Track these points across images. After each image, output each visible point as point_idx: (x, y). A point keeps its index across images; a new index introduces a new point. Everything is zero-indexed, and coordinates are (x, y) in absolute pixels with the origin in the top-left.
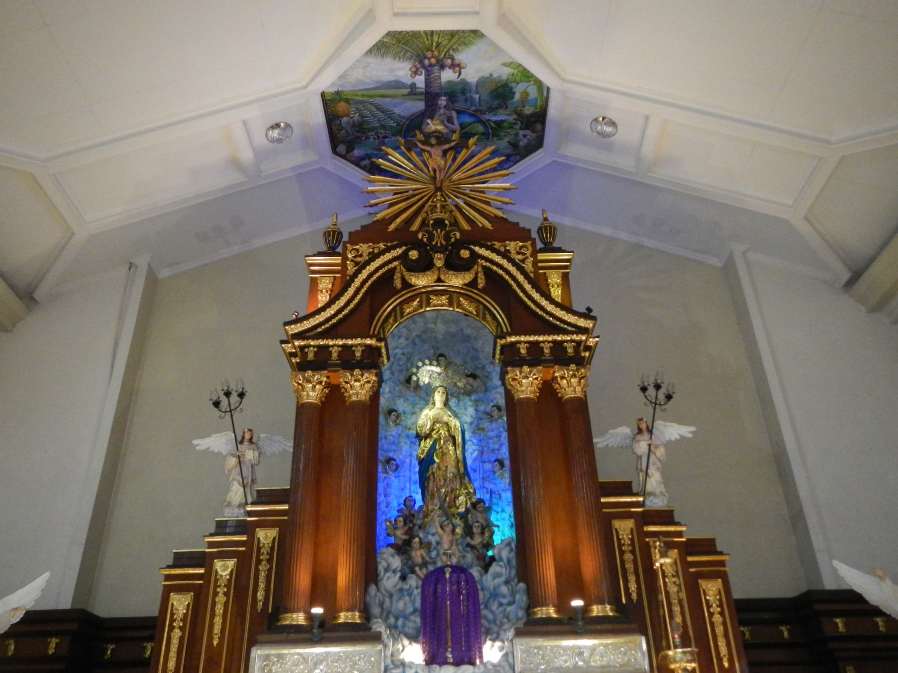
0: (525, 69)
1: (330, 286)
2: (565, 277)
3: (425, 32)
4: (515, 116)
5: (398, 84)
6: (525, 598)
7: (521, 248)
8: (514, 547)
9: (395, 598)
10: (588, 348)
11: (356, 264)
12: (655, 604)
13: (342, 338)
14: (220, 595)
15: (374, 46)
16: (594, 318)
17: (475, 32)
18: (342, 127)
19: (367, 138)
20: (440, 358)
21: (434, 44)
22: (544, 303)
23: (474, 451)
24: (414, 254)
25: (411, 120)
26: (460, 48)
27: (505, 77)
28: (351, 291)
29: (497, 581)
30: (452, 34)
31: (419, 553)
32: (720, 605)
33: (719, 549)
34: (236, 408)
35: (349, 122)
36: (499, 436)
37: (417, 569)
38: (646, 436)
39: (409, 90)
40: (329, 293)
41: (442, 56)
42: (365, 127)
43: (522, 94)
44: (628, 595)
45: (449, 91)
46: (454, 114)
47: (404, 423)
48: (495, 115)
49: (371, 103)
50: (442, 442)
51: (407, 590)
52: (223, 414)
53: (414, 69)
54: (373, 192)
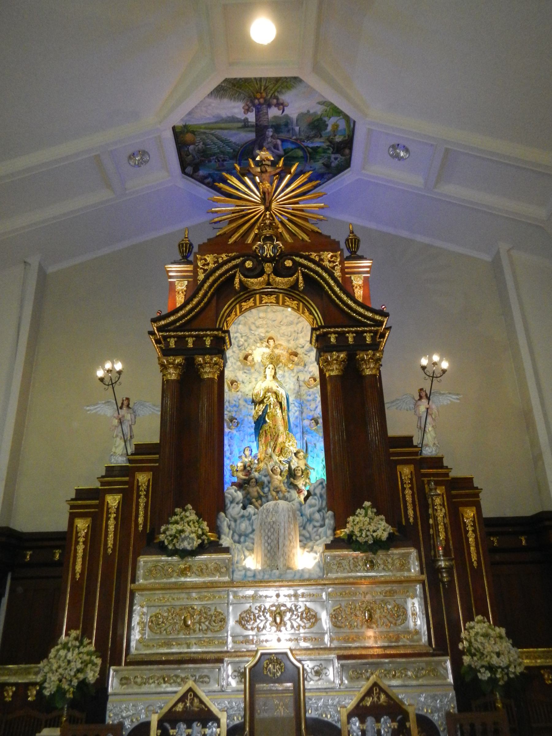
0: (336, 107)
1: (185, 289)
2: (366, 280)
3: (255, 79)
4: (328, 143)
5: (233, 119)
6: (332, 522)
7: (332, 257)
8: (325, 486)
9: (238, 522)
11: (205, 270)
12: (426, 526)
14: (112, 519)
15: (214, 90)
17: (295, 78)
18: (189, 153)
19: (210, 161)
20: (269, 340)
21: (263, 87)
23: (296, 411)
24: (249, 264)
25: (246, 147)
26: (284, 91)
27: (319, 113)
29: (312, 509)
30: (277, 80)
31: (255, 489)
32: (474, 526)
34: (116, 382)
35: (195, 149)
37: (254, 500)
38: (424, 401)
39: (243, 124)
40: (184, 293)
41: (269, 97)
42: (208, 153)
43: (333, 126)
44: (407, 519)
45: (274, 124)
46: (279, 142)
48: (312, 143)
49: (212, 134)
50: (272, 406)
51: (247, 517)
52: (107, 387)
53: (247, 108)
54: (216, 212)
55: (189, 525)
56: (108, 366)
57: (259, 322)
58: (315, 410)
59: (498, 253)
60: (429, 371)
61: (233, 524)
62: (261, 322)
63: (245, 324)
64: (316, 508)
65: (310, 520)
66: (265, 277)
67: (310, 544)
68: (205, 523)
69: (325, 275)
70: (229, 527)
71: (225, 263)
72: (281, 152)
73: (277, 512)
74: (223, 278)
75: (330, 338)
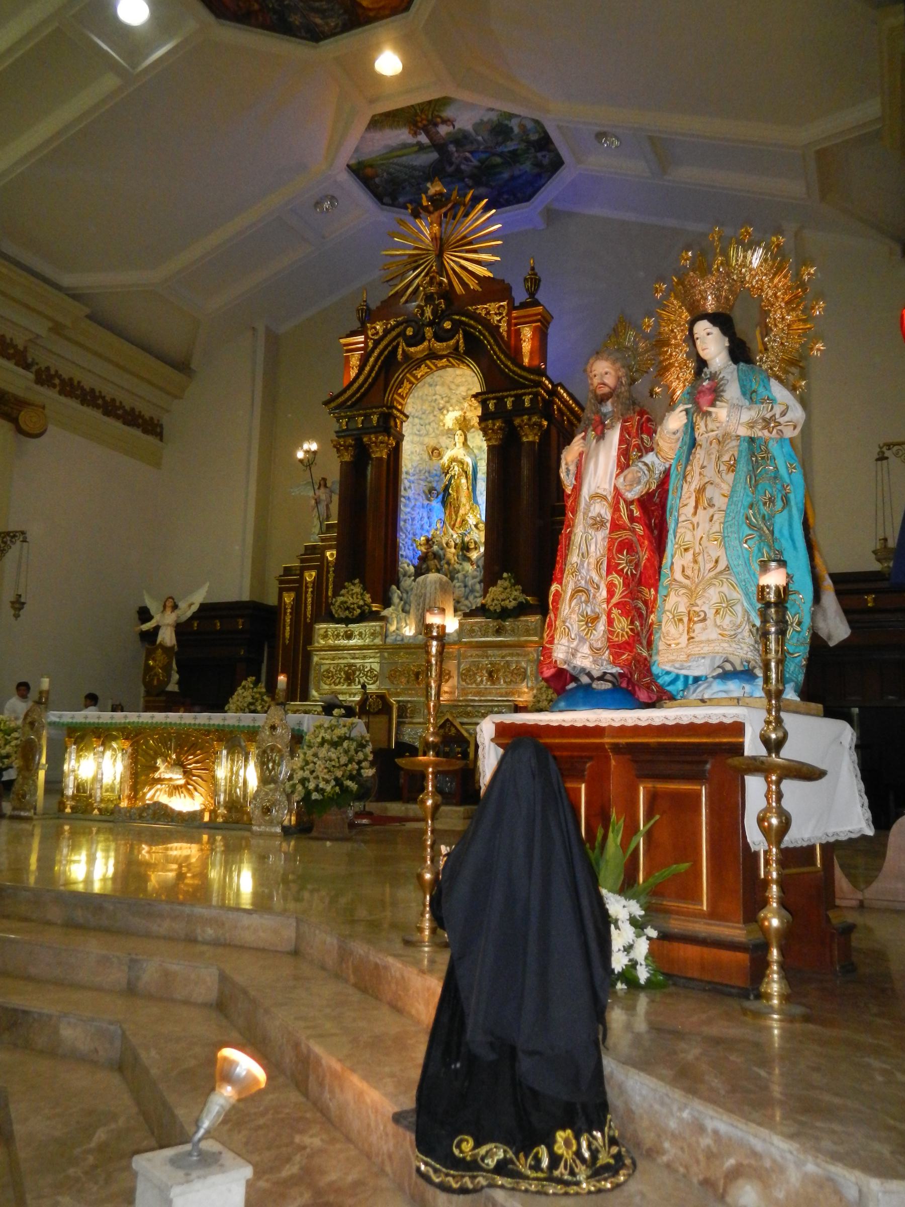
4: (525, 144)
5: (405, 146)
7: (499, 308)
19: (404, 188)
24: (410, 332)
27: (495, 118)
28: (367, 368)
29: (475, 580)
30: (430, 102)
31: (432, 562)
41: (430, 117)
46: (468, 154)
49: (391, 163)
50: (456, 477)
53: (412, 132)
55: (352, 598)
57: (458, 380)
61: (405, 596)
62: (460, 380)
63: (443, 385)
64: (478, 580)
65: (472, 591)
66: (426, 343)
68: (368, 596)
70: (401, 599)
71: (393, 328)
72: (475, 163)
73: (425, 584)
74: (390, 348)
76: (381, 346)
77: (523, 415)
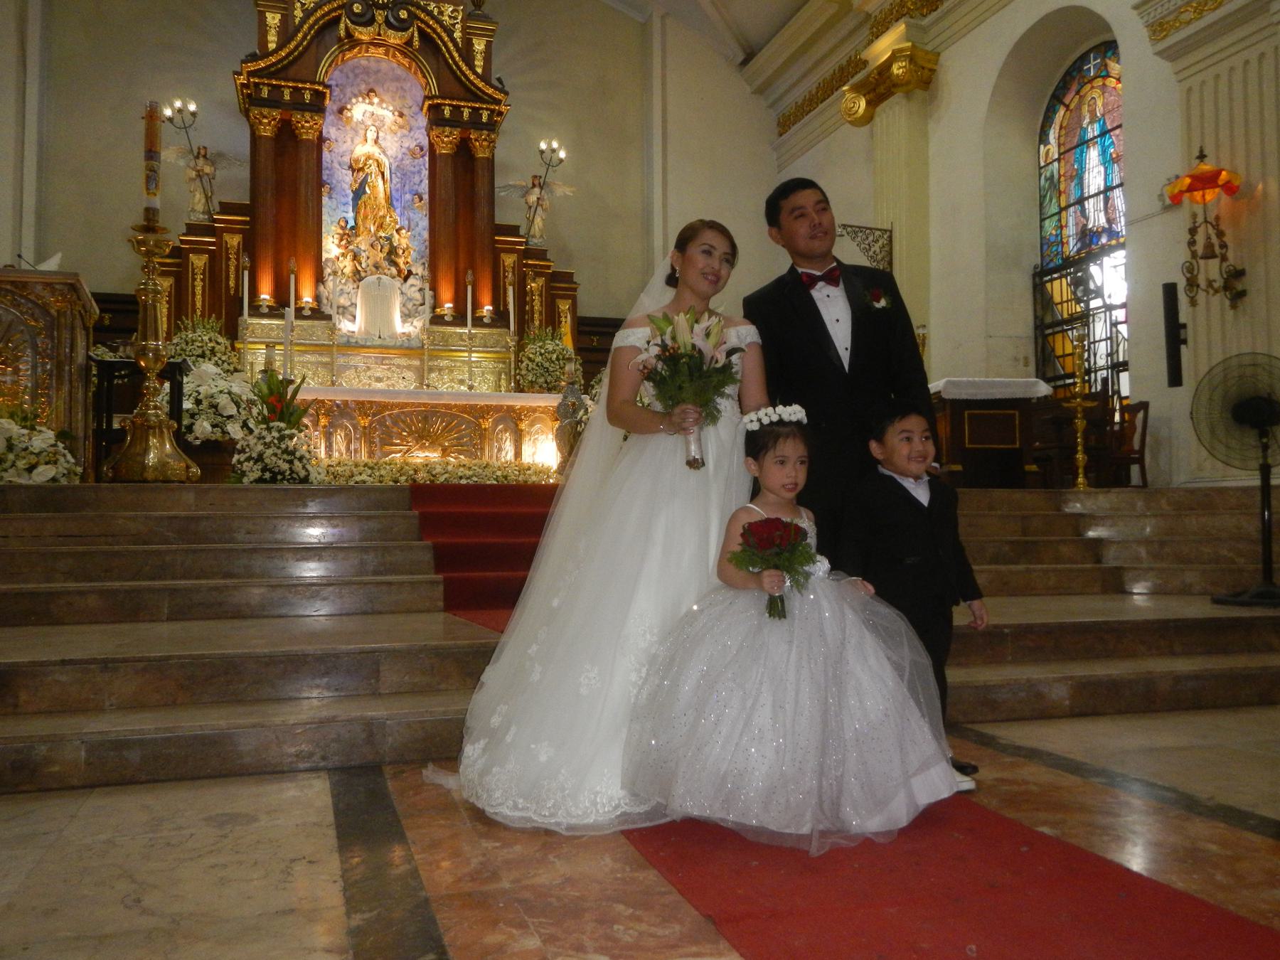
2: (489, 45)
7: (452, 12)
10: (500, 114)
13: (294, 81)
14: (198, 280)
16: (506, 93)
22: (468, 72)
24: (357, 8)
28: (300, 35)
33: (575, 280)
34: (190, 126)
36: (419, 172)
38: (537, 190)
47: (336, 150)
50: (373, 176)
56: (178, 104)
58: (419, 185)
59: (651, 16)
60: (547, 156)
64: (417, 288)
67: (410, 320)
69: (444, 35)
75: (444, 110)
76: (319, 14)
77: (482, 130)
